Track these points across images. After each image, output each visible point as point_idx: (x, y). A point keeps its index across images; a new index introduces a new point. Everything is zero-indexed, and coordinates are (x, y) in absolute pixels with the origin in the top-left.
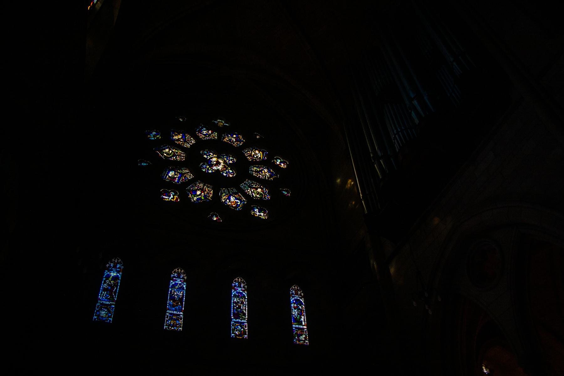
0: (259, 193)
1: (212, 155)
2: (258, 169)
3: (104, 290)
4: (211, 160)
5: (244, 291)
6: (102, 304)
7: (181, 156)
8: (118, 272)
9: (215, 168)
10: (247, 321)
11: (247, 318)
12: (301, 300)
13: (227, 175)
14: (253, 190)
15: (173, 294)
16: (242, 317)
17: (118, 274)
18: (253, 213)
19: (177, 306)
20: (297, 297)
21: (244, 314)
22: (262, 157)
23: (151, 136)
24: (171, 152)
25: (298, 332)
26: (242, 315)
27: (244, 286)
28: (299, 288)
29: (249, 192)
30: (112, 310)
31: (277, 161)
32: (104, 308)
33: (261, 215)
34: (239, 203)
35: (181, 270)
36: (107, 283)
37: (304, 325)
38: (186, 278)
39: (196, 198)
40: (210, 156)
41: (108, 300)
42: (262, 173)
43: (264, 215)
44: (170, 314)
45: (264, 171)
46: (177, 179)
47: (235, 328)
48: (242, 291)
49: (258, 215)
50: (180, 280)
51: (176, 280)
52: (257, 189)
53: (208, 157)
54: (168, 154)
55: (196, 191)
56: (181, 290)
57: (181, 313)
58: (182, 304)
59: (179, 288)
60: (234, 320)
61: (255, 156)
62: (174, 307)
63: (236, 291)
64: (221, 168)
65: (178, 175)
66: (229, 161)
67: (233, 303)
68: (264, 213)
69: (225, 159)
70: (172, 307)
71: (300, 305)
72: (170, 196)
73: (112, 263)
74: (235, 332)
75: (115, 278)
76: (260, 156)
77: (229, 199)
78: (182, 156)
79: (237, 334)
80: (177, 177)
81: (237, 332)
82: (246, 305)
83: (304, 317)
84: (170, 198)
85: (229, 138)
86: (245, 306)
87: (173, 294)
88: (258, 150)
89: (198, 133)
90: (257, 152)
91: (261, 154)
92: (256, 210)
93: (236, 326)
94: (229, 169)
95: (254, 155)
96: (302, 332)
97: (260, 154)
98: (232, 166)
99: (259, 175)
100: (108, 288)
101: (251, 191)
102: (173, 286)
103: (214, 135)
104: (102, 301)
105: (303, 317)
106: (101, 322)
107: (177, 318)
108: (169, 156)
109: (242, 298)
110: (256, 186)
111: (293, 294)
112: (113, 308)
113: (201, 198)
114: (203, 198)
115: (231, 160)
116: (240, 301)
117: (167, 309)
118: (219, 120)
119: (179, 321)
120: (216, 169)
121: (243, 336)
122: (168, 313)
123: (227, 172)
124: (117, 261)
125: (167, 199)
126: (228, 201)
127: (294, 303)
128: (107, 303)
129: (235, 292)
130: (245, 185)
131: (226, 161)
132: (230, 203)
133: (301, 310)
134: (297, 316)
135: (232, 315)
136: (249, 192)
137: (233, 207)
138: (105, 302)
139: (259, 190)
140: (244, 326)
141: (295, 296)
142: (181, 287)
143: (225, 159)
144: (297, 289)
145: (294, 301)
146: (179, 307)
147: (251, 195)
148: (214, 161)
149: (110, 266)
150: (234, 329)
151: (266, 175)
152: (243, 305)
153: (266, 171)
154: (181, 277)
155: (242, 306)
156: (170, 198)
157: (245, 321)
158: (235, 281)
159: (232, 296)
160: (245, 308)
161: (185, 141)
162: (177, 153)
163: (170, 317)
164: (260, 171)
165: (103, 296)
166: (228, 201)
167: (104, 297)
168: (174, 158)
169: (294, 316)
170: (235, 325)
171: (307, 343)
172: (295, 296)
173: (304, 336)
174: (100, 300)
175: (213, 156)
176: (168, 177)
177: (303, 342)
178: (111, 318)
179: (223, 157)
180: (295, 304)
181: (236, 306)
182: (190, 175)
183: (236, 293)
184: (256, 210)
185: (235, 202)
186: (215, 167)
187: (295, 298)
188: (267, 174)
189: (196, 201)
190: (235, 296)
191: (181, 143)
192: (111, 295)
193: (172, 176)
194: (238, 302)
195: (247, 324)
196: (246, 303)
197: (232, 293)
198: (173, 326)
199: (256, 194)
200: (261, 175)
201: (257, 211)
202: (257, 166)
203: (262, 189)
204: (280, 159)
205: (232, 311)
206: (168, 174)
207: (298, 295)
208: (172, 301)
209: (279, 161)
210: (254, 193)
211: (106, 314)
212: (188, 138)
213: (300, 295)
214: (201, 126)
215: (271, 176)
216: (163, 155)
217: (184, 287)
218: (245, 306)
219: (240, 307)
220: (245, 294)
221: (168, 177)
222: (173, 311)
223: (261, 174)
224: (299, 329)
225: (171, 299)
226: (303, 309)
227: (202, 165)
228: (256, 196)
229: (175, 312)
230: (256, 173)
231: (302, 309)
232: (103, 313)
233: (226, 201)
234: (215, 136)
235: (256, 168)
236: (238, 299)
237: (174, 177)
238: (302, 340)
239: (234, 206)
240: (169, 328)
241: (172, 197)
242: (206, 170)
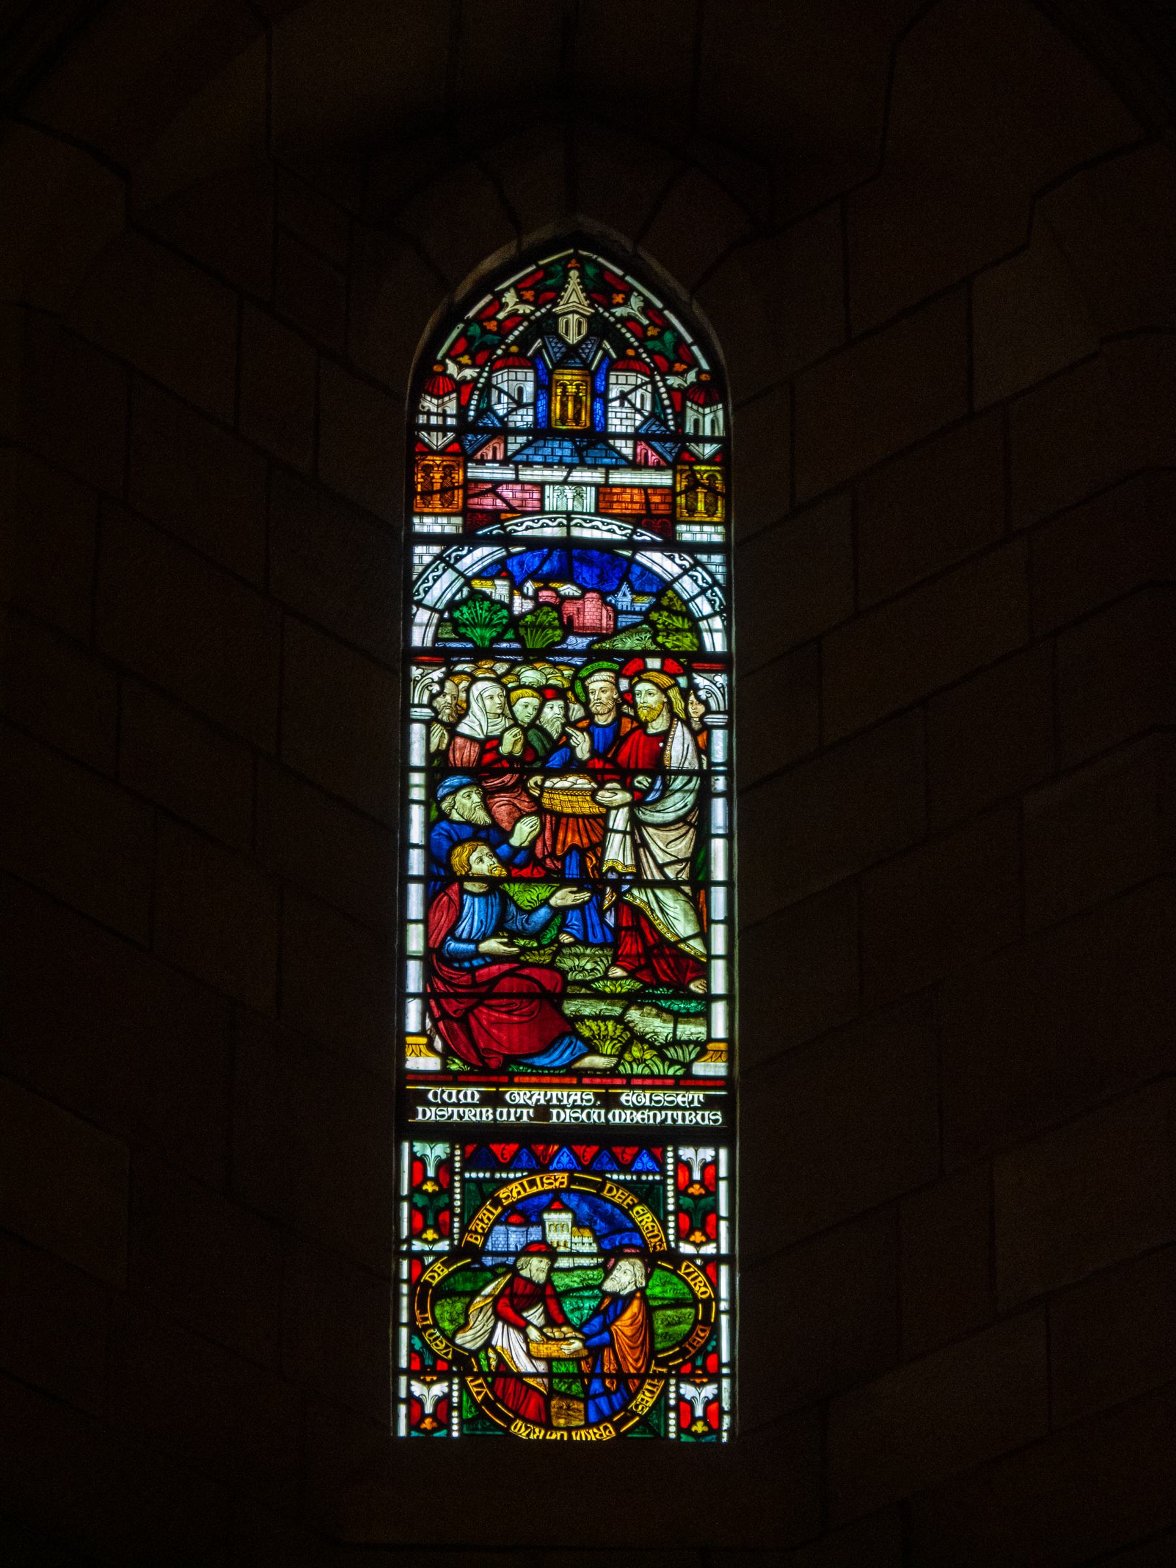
26: (631, 999)
27: (656, 416)
63: (506, 540)
67: (431, 787)
74: (467, 1340)
79: (524, 1364)
81: (522, 1327)
82: (704, 797)
86: (677, 804)
93: (488, 1214)
116: (589, 724)
129: (476, 558)
152: (639, 801)
155: (619, 820)
159: (420, 637)
160: (683, 847)
183: (490, 573)
196: (704, 750)
205: (415, 940)
236: (545, 693)
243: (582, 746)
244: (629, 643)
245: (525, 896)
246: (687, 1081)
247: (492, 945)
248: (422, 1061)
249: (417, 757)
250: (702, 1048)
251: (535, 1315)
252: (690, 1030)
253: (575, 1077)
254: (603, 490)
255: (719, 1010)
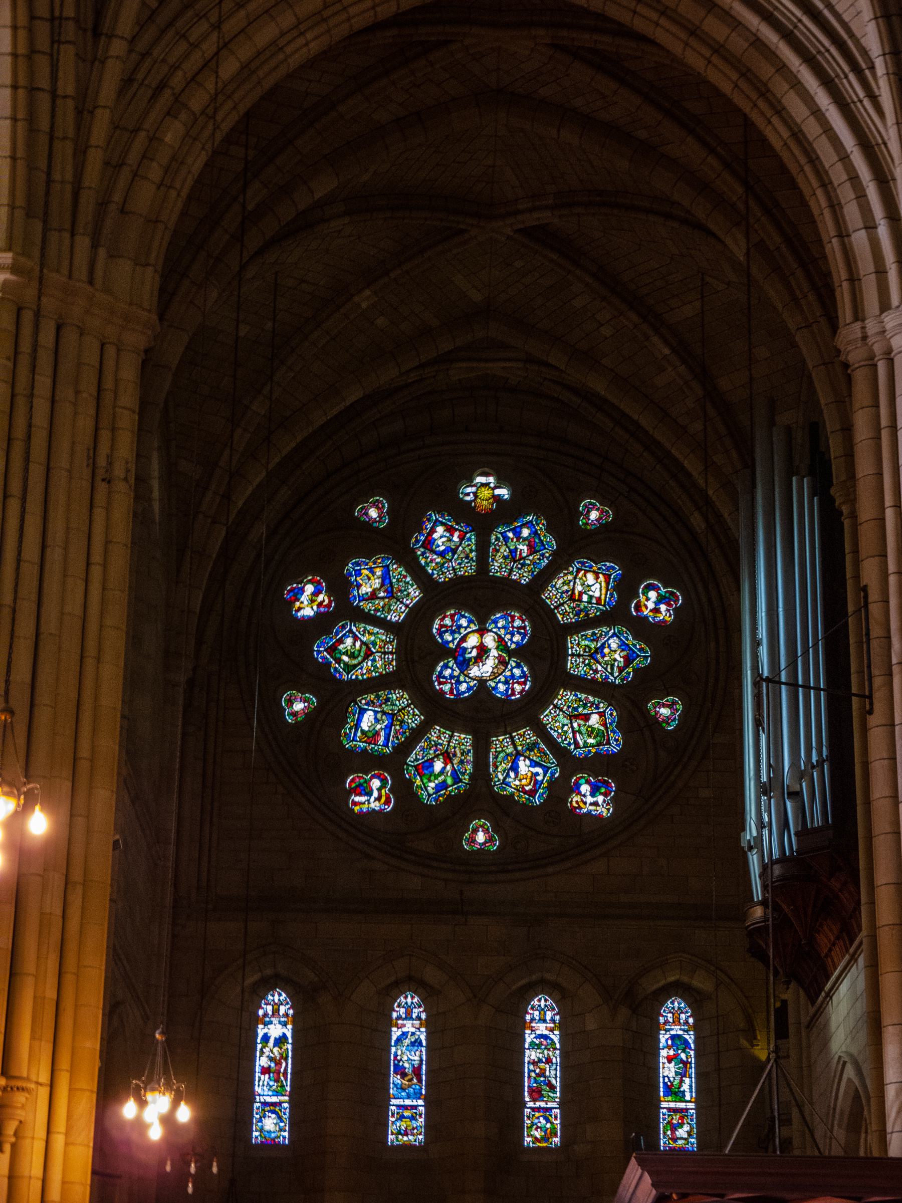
0: (593, 729)
1: (466, 628)
2: (593, 646)
3: (265, 1071)
4: (464, 645)
5: (552, 1030)
6: (265, 1104)
7: (385, 653)
8: (285, 1024)
9: (475, 671)
10: (560, 1103)
11: (560, 1098)
12: (687, 1037)
13: (507, 690)
14: (579, 725)
15: (401, 1060)
16: (549, 1096)
17: (285, 1031)
18: (577, 802)
19: (410, 1086)
20: (677, 1030)
21: (552, 1088)
22: (603, 597)
23: (302, 603)
24: (358, 644)
25: (673, 1119)
28: (683, 1005)
29: (566, 732)
30: (285, 1114)
31: (648, 599)
32: (269, 1111)
33: (596, 804)
34: (539, 778)
35: (413, 998)
36: (267, 1054)
37: (690, 1102)
38: (423, 1016)
39: (432, 785)
40: (460, 634)
41: (275, 1093)
42: (603, 656)
43: (604, 801)
44: (399, 1107)
45: (609, 646)
46: (382, 733)
47: (533, 1124)
48: (546, 1032)
49: (591, 804)
50: (413, 1024)
51: (404, 1026)
52: (586, 718)
53: (456, 636)
54: (352, 656)
55: (431, 762)
56: (416, 1048)
57: (421, 1102)
58: (420, 1080)
59: (413, 1044)
60: (531, 1104)
61: (585, 598)
62: (403, 1089)
64: (490, 670)
65: (383, 722)
66: (513, 635)
68: (605, 795)
69: (502, 632)
70: (400, 1090)
71: (684, 1051)
72: (370, 794)
73: (270, 1004)
74: (532, 1133)
75: (281, 1041)
76: (597, 594)
77: (515, 768)
78: (388, 653)
79: (538, 1137)
80: (381, 729)
83: (691, 1081)
84: (372, 799)
85: (509, 548)
86: (554, 1067)
87: (401, 1060)
88: (594, 572)
89: (423, 554)
90: (590, 578)
91: (600, 584)
92: (585, 788)
94: (514, 664)
95: (581, 594)
96: (682, 1118)
97: (597, 585)
98: (520, 653)
99: (594, 667)
100: (270, 1066)
101: (572, 727)
102: (399, 1040)
103: (469, 545)
104: (263, 1095)
105: (687, 1080)
106: (270, 1145)
107: (412, 1115)
108: (355, 662)
109: (549, 1050)
110: (584, 708)
111: (667, 1022)
112: (285, 1109)
113: (444, 782)
114: (449, 781)
115: (518, 633)
117: (391, 1096)
118: (480, 479)
119: (416, 1120)
120: (478, 674)
121: (550, 1140)
122: (393, 1105)
123: (505, 677)
124: (279, 1000)
125: (364, 803)
126: (512, 774)
127: (669, 1047)
128: (275, 1099)
130: (555, 712)
131: (503, 639)
132: (517, 783)
133: (685, 1063)
134: (674, 1079)
135: (526, 1094)
136: (566, 732)
137: (525, 792)
138: (268, 1099)
139: (594, 720)
140: (551, 1116)
141: (673, 1027)
142: (416, 1040)
143: (502, 632)
144: (679, 1008)
145: (670, 1042)
146: (414, 1089)
147: (572, 741)
148: (473, 648)
149: (266, 1015)
150: (531, 1127)
151: (615, 660)
153: (614, 646)
154: (414, 1016)
155: (548, 1069)
156: (372, 799)
157: (555, 1105)
158: (532, 1009)
159: (527, 1046)
160: (554, 1072)
161: (391, 595)
162: (374, 644)
163: (398, 1113)
164: (597, 650)
165: (263, 1085)
166: (512, 774)
167: (265, 1088)
168: (370, 663)
169: (666, 1080)
170: (533, 1115)
171: (692, 1144)
172: (673, 1027)
173: (686, 1128)
174: (259, 1095)
175: (469, 630)
176: (359, 734)
177: (683, 1141)
178: (285, 1131)
179: (496, 627)
180: (669, 1049)
181: (534, 1071)
182: (414, 715)
184: (585, 788)
185: (529, 774)
186: (476, 668)
187: (673, 1032)
188: (617, 656)
189: (434, 793)
190: (532, 1043)
191: (382, 604)
192: (277, 1080)
193: (369, 727)
194: (540, 1061)
195: (558, 1111)
197: (524, 1040)
198: (406, 1134)
199: (586, 736)
200: (600, 664)
201: (588, 793)
202: (590, 632)
203: (602, 714)
204: (656, 589)
206: (357, 726)
207: (680, 1024)
208: (399, 1077)
209: (653, 595)
210: (580, 733)
211: (276, 1124)
212: (398, 579)
213: (687, 1023)
214: (429, 520)
215: (628, 660)
216: (338, 661)
217: (421, 1040)
218: (554, 1067)
219: (542, 1073)
220: (555, 1037)
221: (359, 734)
222: (403, 1099)
223: (601, 660)
224: (676, 1111)
225: (396, 1072)
226: (689, 1060)
227: (441, 672)
228: (585, 741)
229: (408, 1102)
230: (587, 662)
231: (687, 1058)
232: (270, 1123)
233: (508, 775)
234: (471, 551)
235: (587, 643)
237: (374, 729)
238: (682, 1138)
239: (527, 788)
240: (397, 1138)
241: (376, 794)
242: (452, 684)
243: (544, 1060)
244: (549, 1047)
245: (538, 1079)
246: (555, 1102)
247: (535, 1085)
248: (527, 1099)
249: (526, 1061)
250: (556, 1097)
251: (539, 1130)
252: (555, 1095)
253: (543, 1101)
254: (546, 1027)
255: (558, 1093)
